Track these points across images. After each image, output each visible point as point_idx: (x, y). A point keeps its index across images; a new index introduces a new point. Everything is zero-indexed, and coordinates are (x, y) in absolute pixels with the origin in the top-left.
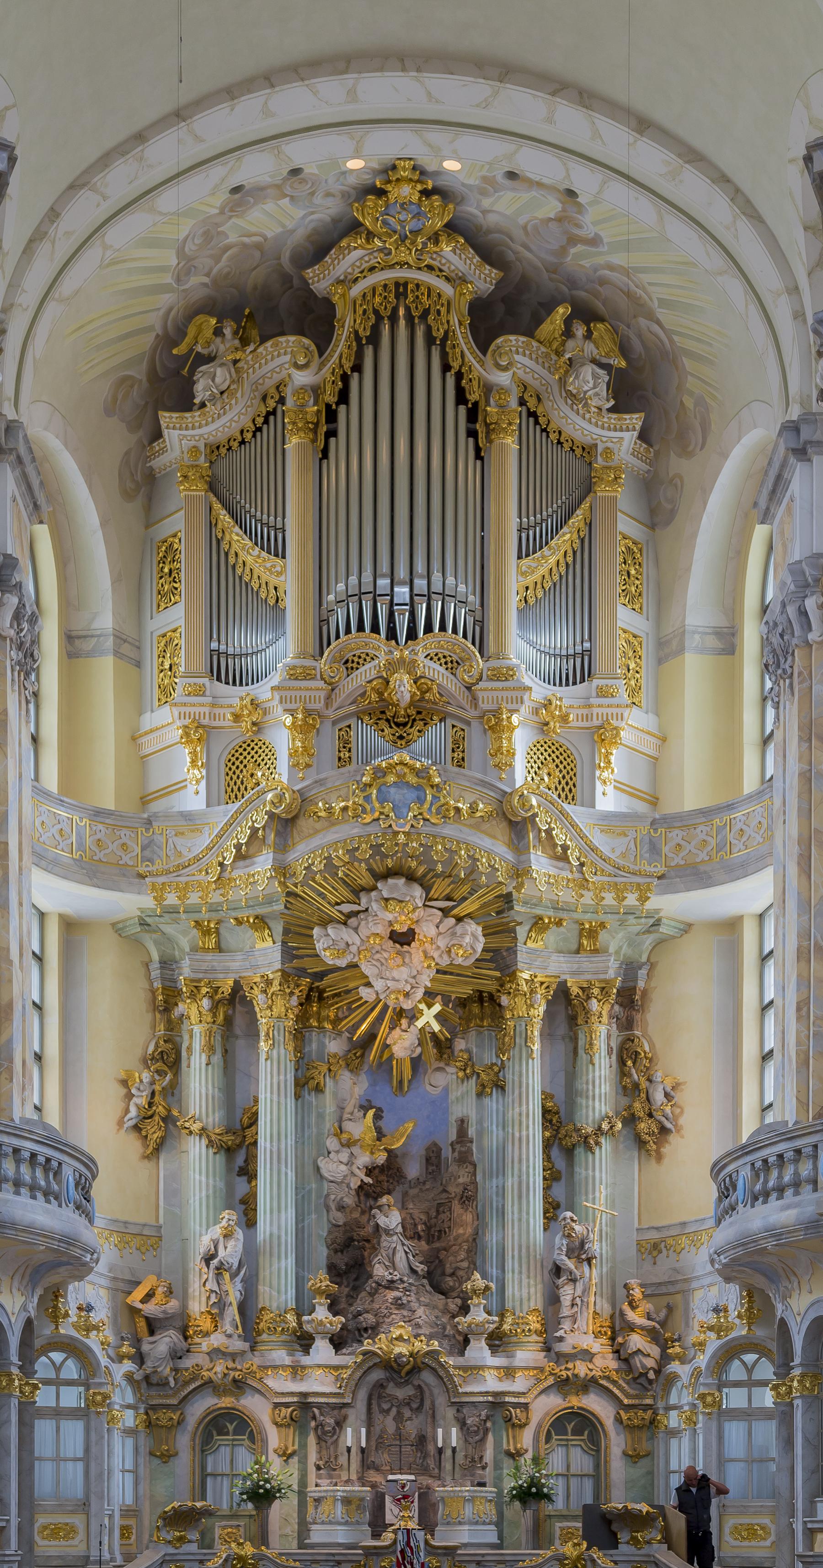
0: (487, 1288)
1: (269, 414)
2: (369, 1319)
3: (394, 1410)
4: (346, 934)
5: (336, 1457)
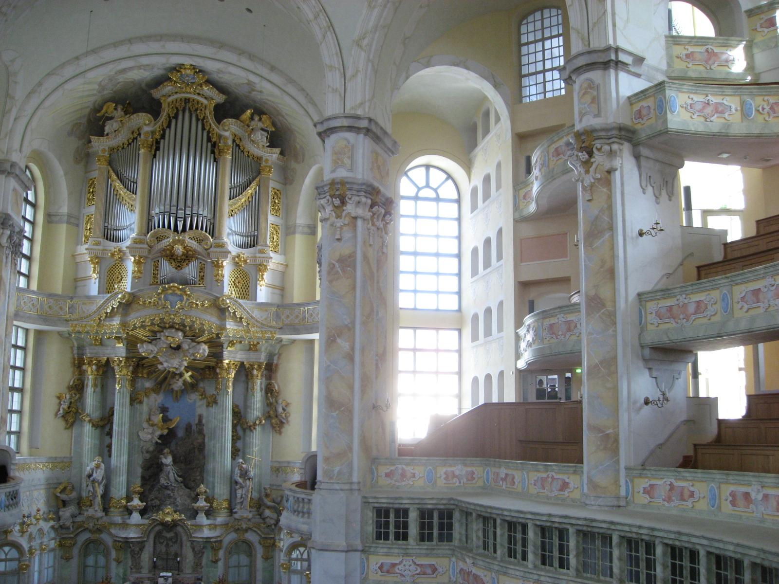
0: (206, 492)
1: (134, 139)
2: (158, 503)
3: (165, 543)
4: (151, 347)
5: (139, 563)
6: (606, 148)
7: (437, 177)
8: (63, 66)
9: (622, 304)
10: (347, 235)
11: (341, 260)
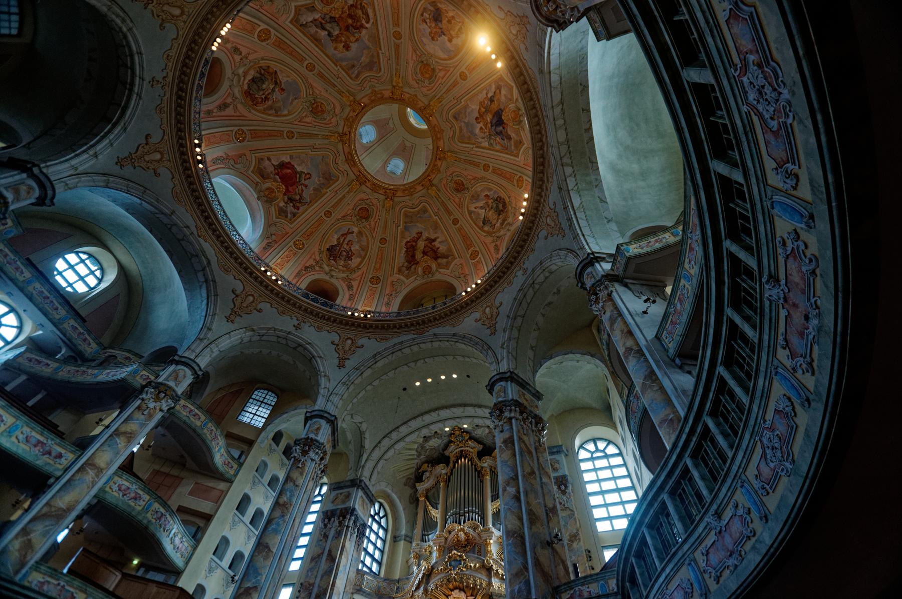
6: (602, 287)
7: (601, 445)
8: (391, 432)
9: (642, 343)
10: (506, 427)
11: (505, 442)
